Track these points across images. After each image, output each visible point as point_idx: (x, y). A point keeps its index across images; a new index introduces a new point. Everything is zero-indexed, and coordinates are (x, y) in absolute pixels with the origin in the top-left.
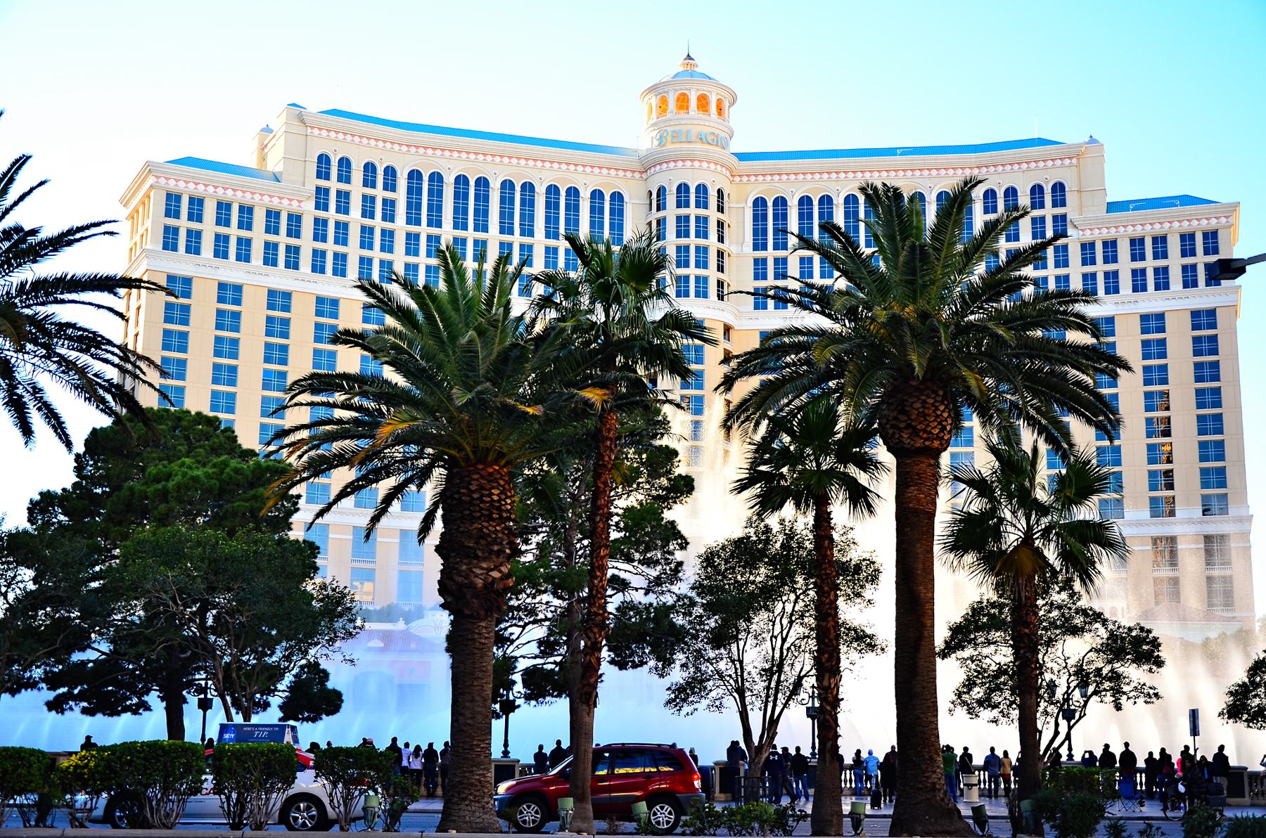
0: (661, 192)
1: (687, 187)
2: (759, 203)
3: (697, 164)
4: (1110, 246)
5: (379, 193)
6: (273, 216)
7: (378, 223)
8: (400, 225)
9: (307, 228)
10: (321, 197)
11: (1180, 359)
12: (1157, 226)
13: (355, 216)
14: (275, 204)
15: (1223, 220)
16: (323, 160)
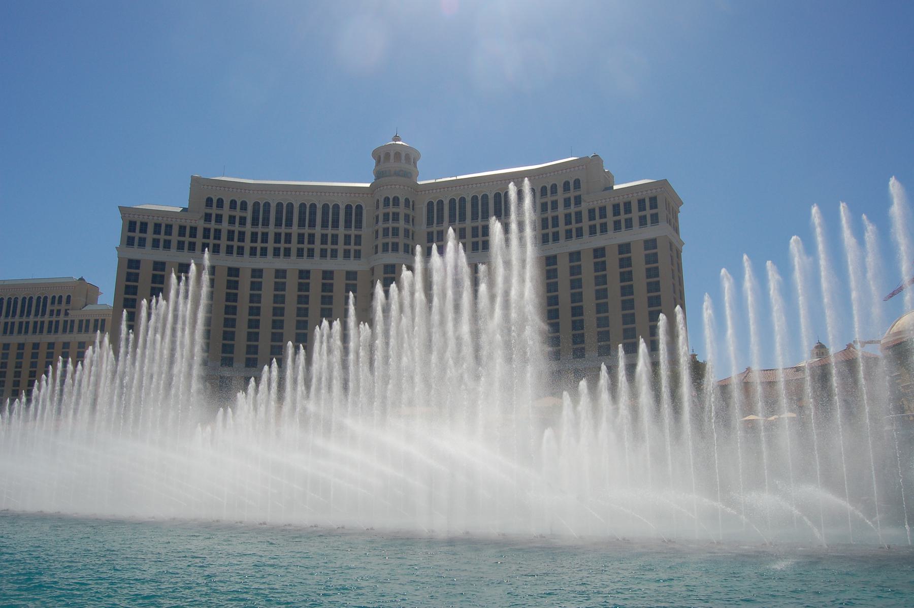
0: (378, 200)
1: (389, 199)
2: (430, 204)
3: (393, 187)
4: (603, 210)
5: (238, 213)
6: (182, 229)
7: (237, 228)
8: (248, 229)
9: (200, 233)
10: (208, 217)
11: (639, 268)
12: (626, 196)
13: (225, 226)
14: (183, 223)
15: (659, 190)
16: (209, 202)
